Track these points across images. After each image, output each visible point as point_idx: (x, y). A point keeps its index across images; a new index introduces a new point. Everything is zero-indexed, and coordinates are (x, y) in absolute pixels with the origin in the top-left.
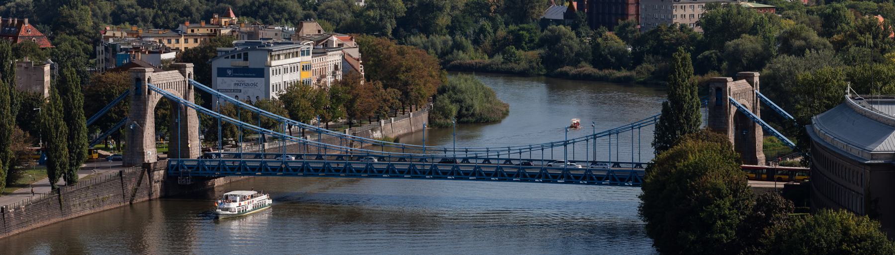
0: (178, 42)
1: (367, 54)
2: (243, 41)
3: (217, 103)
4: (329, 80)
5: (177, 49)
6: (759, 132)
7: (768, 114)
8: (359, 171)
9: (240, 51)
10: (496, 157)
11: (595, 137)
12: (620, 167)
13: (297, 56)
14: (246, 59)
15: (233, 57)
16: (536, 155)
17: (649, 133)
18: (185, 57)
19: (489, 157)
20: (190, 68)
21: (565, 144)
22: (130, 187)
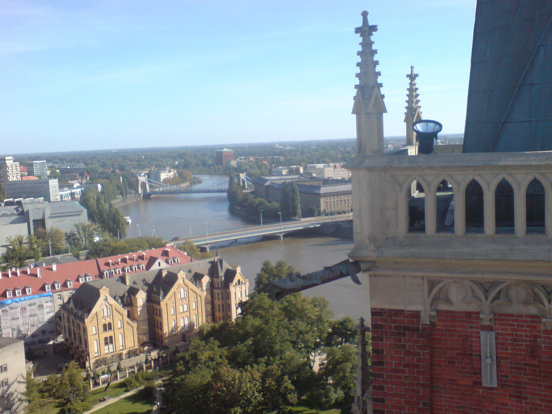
1: (178, 172)
4: (171, 177)
6: (246, 183)
7: (247, 179)
18: (145, 174)
20: (146, 176)
22: (137, 198)
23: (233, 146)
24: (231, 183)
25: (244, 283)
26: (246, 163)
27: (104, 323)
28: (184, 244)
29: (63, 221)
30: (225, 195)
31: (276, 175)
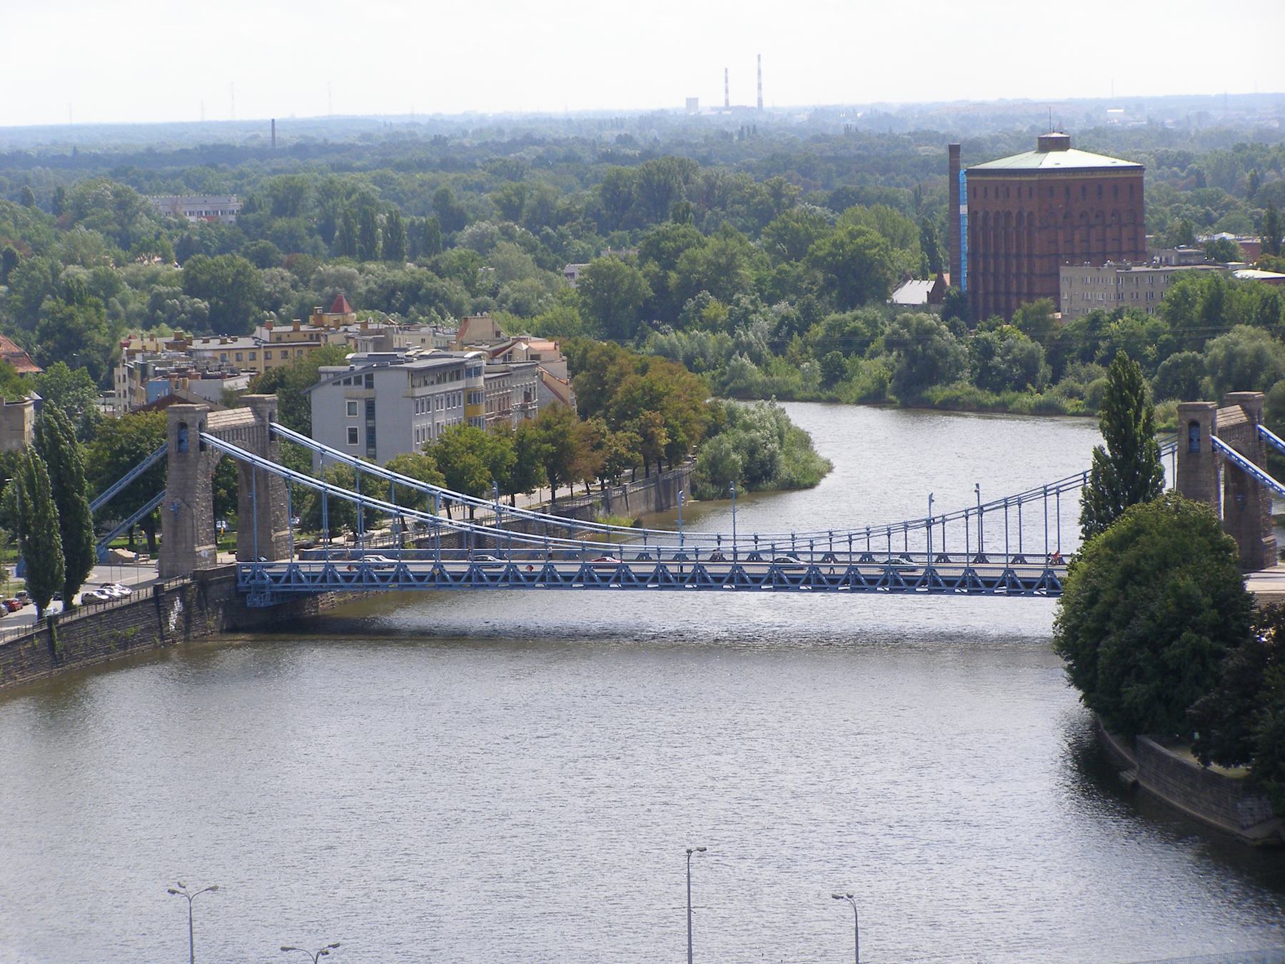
2: (365, 355)
8: (568, 578)
9: (358, 372)
10: (808, 549)
11: (981, 510)
12: (1026, 563)
13: (458, 379)
14: (370, 385)
15: (347, 382)
16: (878, 544)
17: (1073, 504)
19: (796, 550)
21: (929, 523)
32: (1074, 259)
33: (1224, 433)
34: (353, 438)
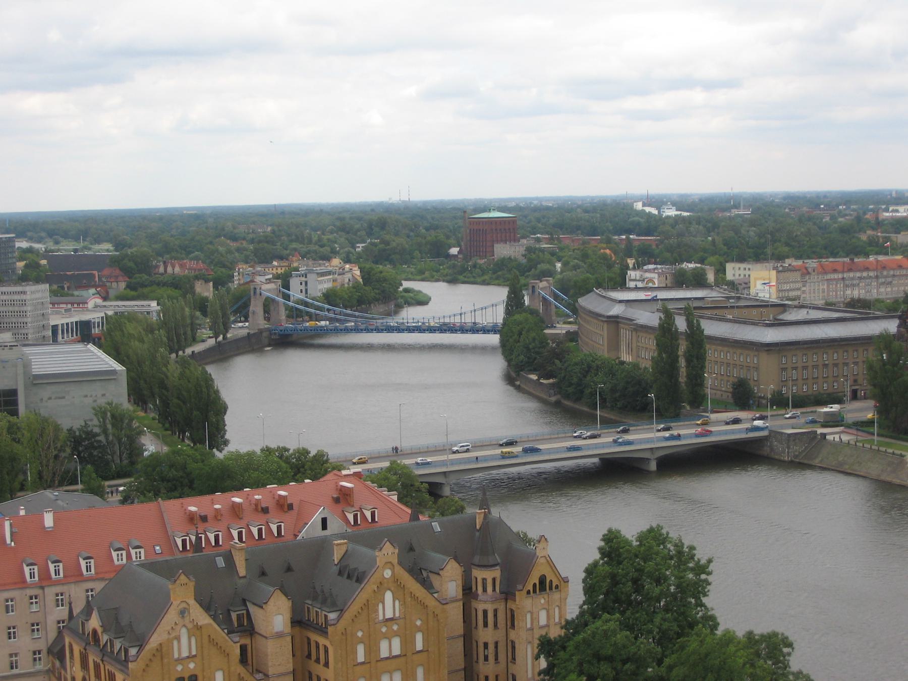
0: (272, 270)
3: (292, 298)
5: (273, 273)
14: (306, 277)
18: (277, 277)
21: (461, 314)
23: (513, 204)
24: (514, 303)
25: (557, 587)
26: (553, 254)
27: (179, 676)
28: (389, 470)
29: (64, 398)
30: (494, 339)
31: (637, 289)
32: (498, 242)
33: (541, 289)
34: (301, 292)
